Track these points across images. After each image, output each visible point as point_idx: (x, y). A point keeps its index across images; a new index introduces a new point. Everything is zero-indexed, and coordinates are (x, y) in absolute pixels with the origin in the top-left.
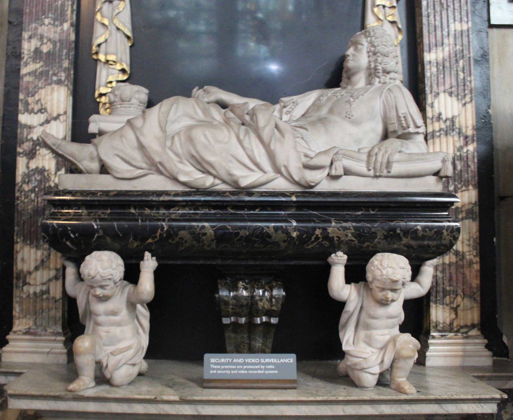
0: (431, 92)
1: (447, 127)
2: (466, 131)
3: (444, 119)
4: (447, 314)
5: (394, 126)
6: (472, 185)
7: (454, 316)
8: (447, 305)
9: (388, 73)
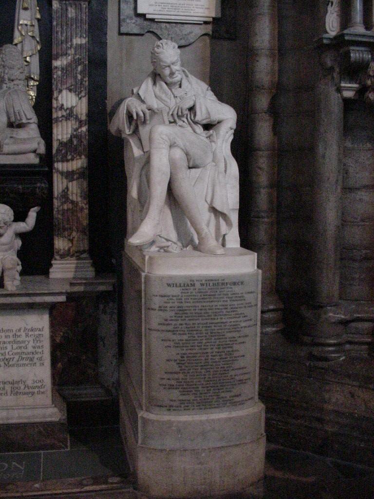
0: (56, 89)
1: (67, 114)
2: (81, 117)
3: (65, 108)
4: (66, 244)
5: (13, 119)
6: (85, 156)
7: (71, 245)
8: (66, 237)
9: (13, 80)
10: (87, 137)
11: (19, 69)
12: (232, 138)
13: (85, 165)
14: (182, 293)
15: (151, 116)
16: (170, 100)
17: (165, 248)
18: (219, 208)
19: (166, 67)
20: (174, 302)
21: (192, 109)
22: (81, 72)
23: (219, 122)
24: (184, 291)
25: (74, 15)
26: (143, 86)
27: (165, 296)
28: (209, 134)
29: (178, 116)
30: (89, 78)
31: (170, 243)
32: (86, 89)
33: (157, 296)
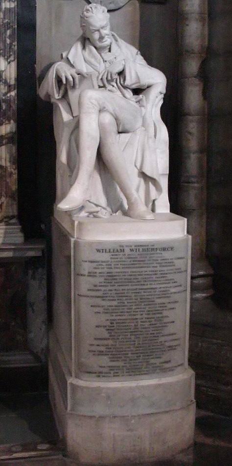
2: (10, 81)
6: (13, 120)
10: (16, 102)
12: (161, 102)
13: (14, 130)
14: (111, 258)
15: (81, 81)
16: (100, 64)
17: (95, 214)
18: (148, 173)
19: (96, 31)
20: (104, 268)
21: (121, 73)
22: (10, 37)
23: (149, 87)
24: (113, 257)
26: (73, 50)
27: (94, 262)
28: (138, 99)
29: (108, 81)
30: (18, 43)
31: (99, 209)
32: (15, 54)
33: (86, 261)
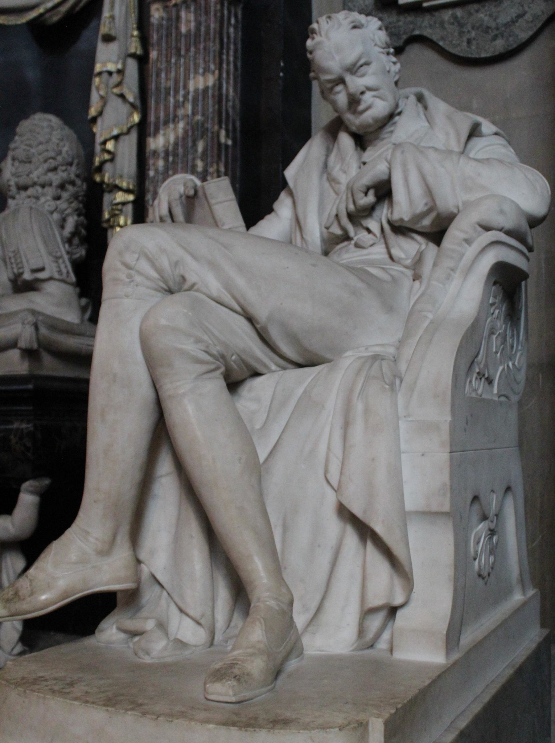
11: (45, 161)
25: (193, 25)
29: (351, 216)
